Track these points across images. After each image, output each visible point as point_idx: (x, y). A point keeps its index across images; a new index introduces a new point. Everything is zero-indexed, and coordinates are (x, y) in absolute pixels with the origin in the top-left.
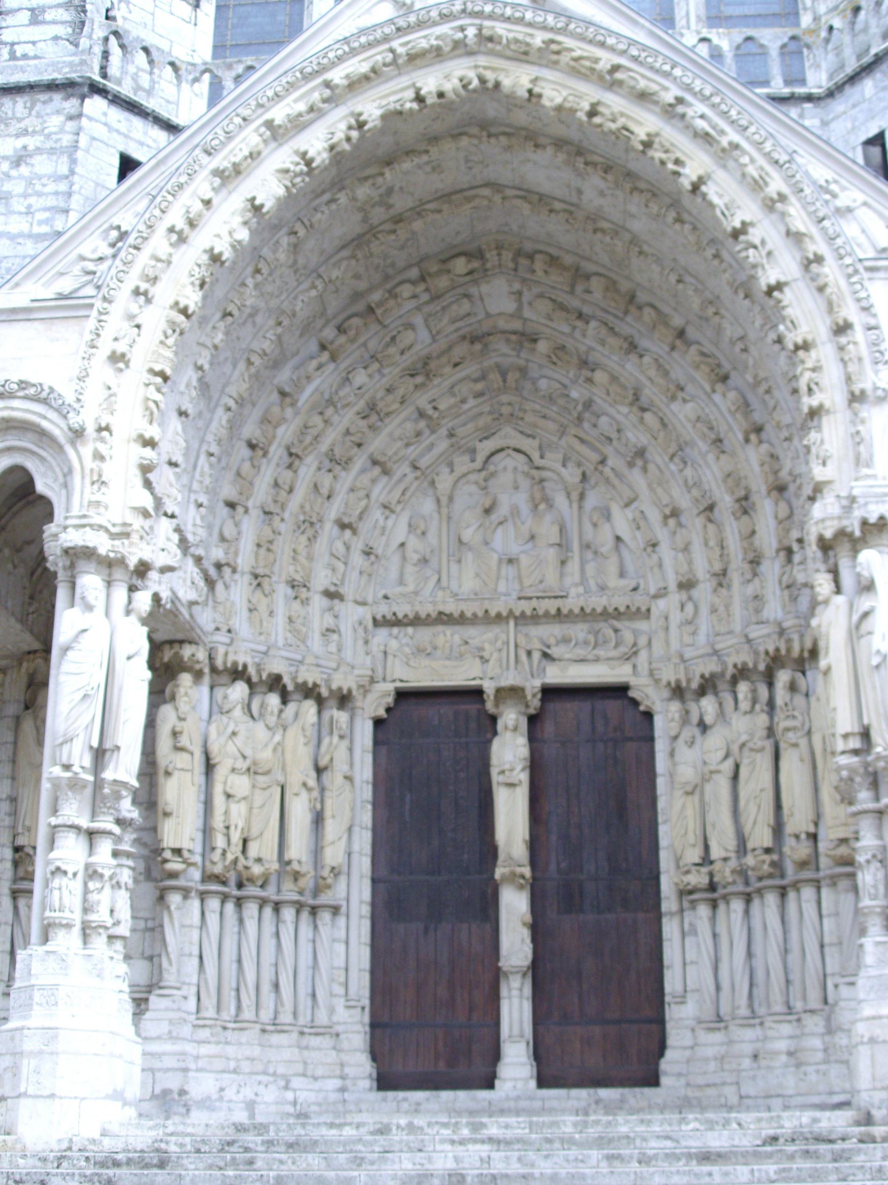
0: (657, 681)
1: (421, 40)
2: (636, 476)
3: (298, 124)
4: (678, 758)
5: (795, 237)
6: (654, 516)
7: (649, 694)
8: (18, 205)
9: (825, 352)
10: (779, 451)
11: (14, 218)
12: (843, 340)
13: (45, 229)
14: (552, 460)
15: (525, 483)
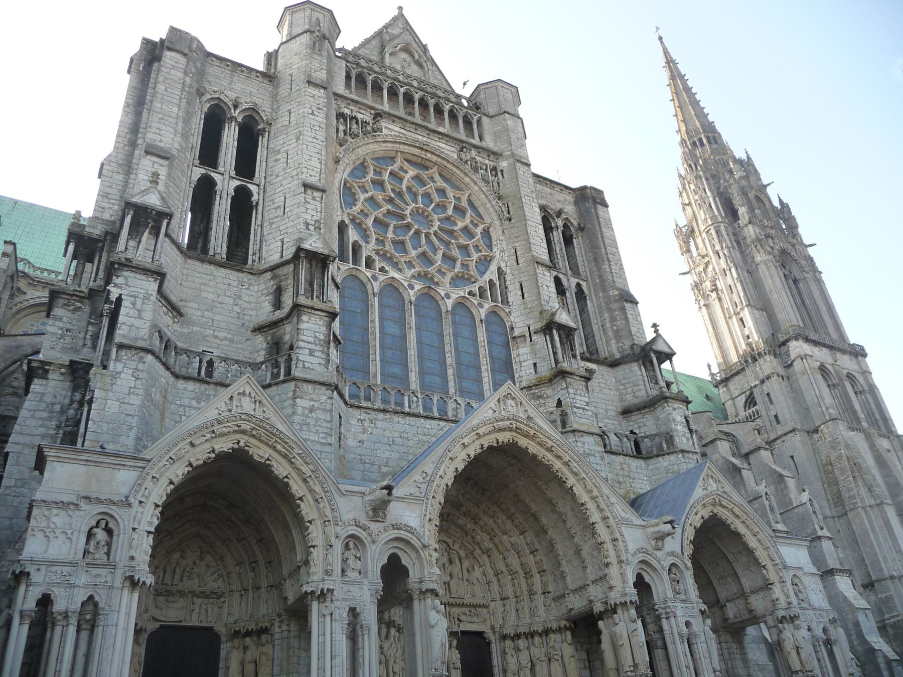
0: (494, 632)
1: (501, 424)
2: (485, 557)
3: (469, 444)
4: (509, 661)
5: (601, 510)
6: (491, 572)
7: (490, 635)
8: (314, 429)
9: (609, 546)
10: (543, 558)
11: (312, 434)
12: (616, 543)
13: (324, 441)
14: (457, 547)
15: (446, 554)
